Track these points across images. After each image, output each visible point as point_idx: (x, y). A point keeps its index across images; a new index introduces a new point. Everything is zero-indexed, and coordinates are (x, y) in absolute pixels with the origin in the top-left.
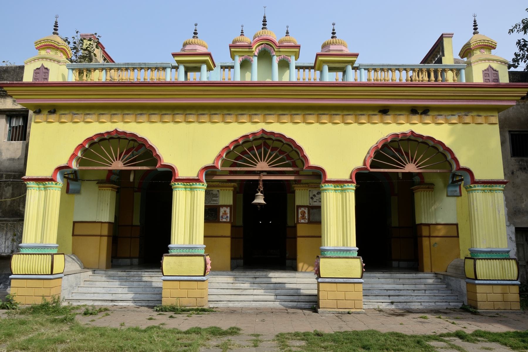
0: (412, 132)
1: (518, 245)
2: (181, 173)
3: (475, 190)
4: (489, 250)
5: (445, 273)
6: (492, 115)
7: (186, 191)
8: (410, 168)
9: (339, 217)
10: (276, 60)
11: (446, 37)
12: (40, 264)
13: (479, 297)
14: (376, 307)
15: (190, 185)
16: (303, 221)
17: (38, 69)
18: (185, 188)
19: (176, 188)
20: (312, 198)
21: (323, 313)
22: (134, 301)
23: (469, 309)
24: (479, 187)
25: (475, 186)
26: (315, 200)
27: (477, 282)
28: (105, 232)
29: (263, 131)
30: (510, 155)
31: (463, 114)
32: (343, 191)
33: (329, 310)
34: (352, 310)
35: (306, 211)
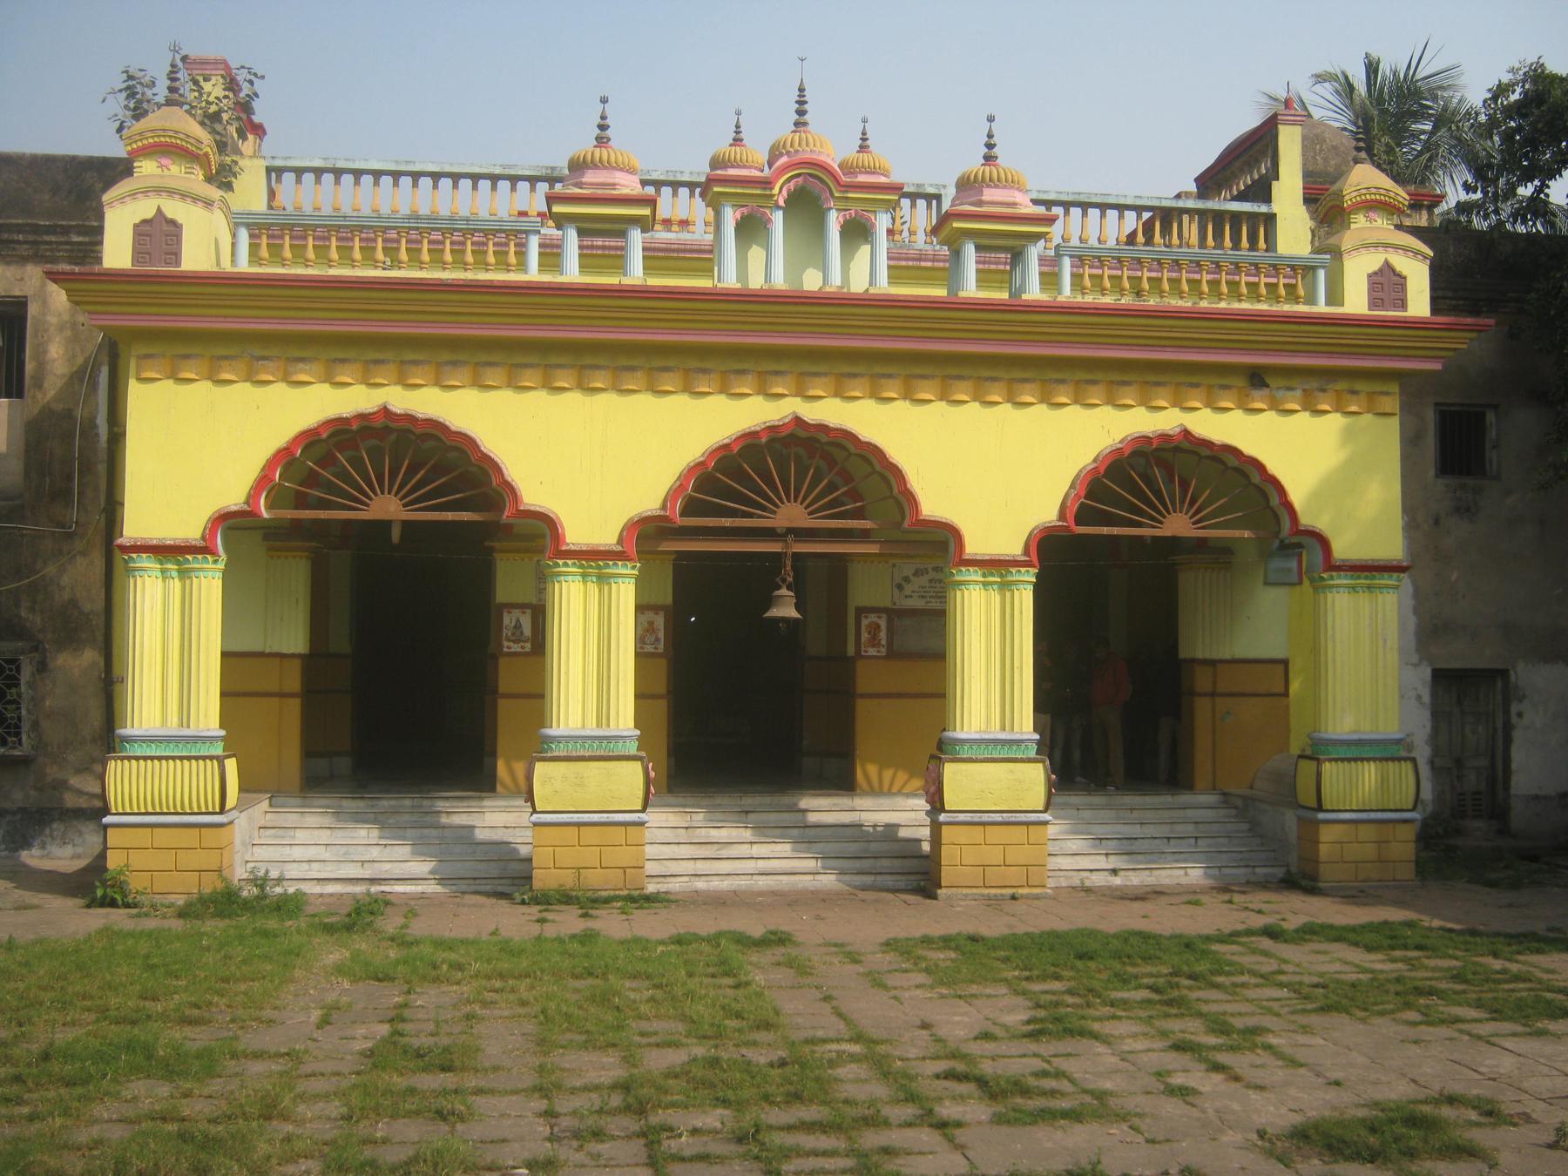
0: (1186, 433)
1: (1435, 715)
2: (576, 534)
3: (1332, 586)
4: (1355, 737)
5: (1248, 792)
6: (1385, 389)
7: (585, 582)
8: (1177, 525)
9: (993, 657)
10: (834, 221)
11: (1286, 123)
12: (190, 784)
13: (1324, 850)
14: (1077, 882)
15: (599, 567)
16: (872, 652)
17: (145, 222)
18: (584, 575)
19: (560, 574)
20: (900, 587)
21: (949, 897)
22: (441, 881)
23: (1301, 879)
24: (1342, 580)
25: (1332, 578)
26: (908, 590)
27: (1321, 816)
28: (294, 683)
29: (798, 421)
30: (1432, 473)
31: (1315, 385)
32: (1005, 586)
33: (965, 891)
34: (1021, 891)
35: (883, 623)
